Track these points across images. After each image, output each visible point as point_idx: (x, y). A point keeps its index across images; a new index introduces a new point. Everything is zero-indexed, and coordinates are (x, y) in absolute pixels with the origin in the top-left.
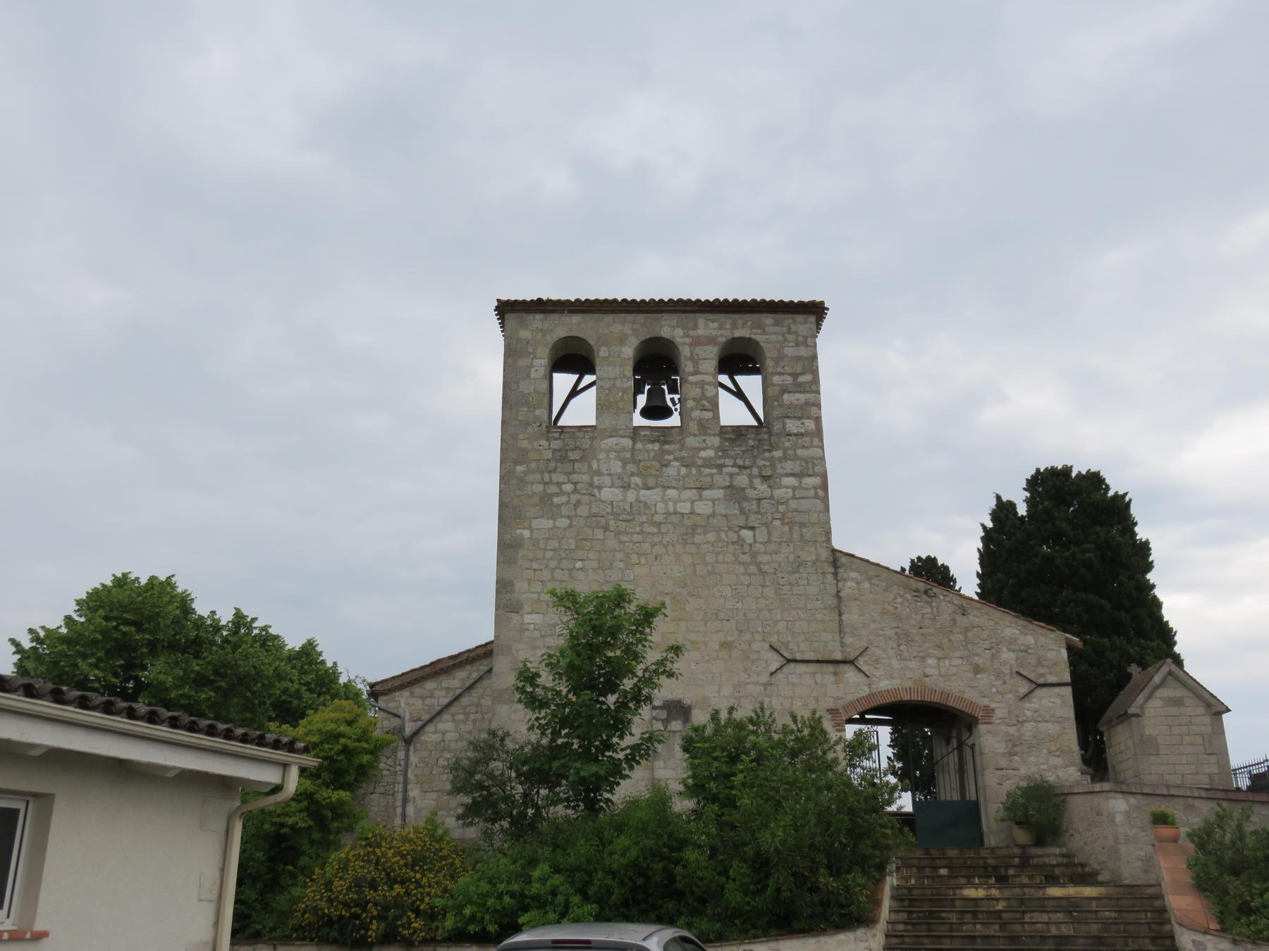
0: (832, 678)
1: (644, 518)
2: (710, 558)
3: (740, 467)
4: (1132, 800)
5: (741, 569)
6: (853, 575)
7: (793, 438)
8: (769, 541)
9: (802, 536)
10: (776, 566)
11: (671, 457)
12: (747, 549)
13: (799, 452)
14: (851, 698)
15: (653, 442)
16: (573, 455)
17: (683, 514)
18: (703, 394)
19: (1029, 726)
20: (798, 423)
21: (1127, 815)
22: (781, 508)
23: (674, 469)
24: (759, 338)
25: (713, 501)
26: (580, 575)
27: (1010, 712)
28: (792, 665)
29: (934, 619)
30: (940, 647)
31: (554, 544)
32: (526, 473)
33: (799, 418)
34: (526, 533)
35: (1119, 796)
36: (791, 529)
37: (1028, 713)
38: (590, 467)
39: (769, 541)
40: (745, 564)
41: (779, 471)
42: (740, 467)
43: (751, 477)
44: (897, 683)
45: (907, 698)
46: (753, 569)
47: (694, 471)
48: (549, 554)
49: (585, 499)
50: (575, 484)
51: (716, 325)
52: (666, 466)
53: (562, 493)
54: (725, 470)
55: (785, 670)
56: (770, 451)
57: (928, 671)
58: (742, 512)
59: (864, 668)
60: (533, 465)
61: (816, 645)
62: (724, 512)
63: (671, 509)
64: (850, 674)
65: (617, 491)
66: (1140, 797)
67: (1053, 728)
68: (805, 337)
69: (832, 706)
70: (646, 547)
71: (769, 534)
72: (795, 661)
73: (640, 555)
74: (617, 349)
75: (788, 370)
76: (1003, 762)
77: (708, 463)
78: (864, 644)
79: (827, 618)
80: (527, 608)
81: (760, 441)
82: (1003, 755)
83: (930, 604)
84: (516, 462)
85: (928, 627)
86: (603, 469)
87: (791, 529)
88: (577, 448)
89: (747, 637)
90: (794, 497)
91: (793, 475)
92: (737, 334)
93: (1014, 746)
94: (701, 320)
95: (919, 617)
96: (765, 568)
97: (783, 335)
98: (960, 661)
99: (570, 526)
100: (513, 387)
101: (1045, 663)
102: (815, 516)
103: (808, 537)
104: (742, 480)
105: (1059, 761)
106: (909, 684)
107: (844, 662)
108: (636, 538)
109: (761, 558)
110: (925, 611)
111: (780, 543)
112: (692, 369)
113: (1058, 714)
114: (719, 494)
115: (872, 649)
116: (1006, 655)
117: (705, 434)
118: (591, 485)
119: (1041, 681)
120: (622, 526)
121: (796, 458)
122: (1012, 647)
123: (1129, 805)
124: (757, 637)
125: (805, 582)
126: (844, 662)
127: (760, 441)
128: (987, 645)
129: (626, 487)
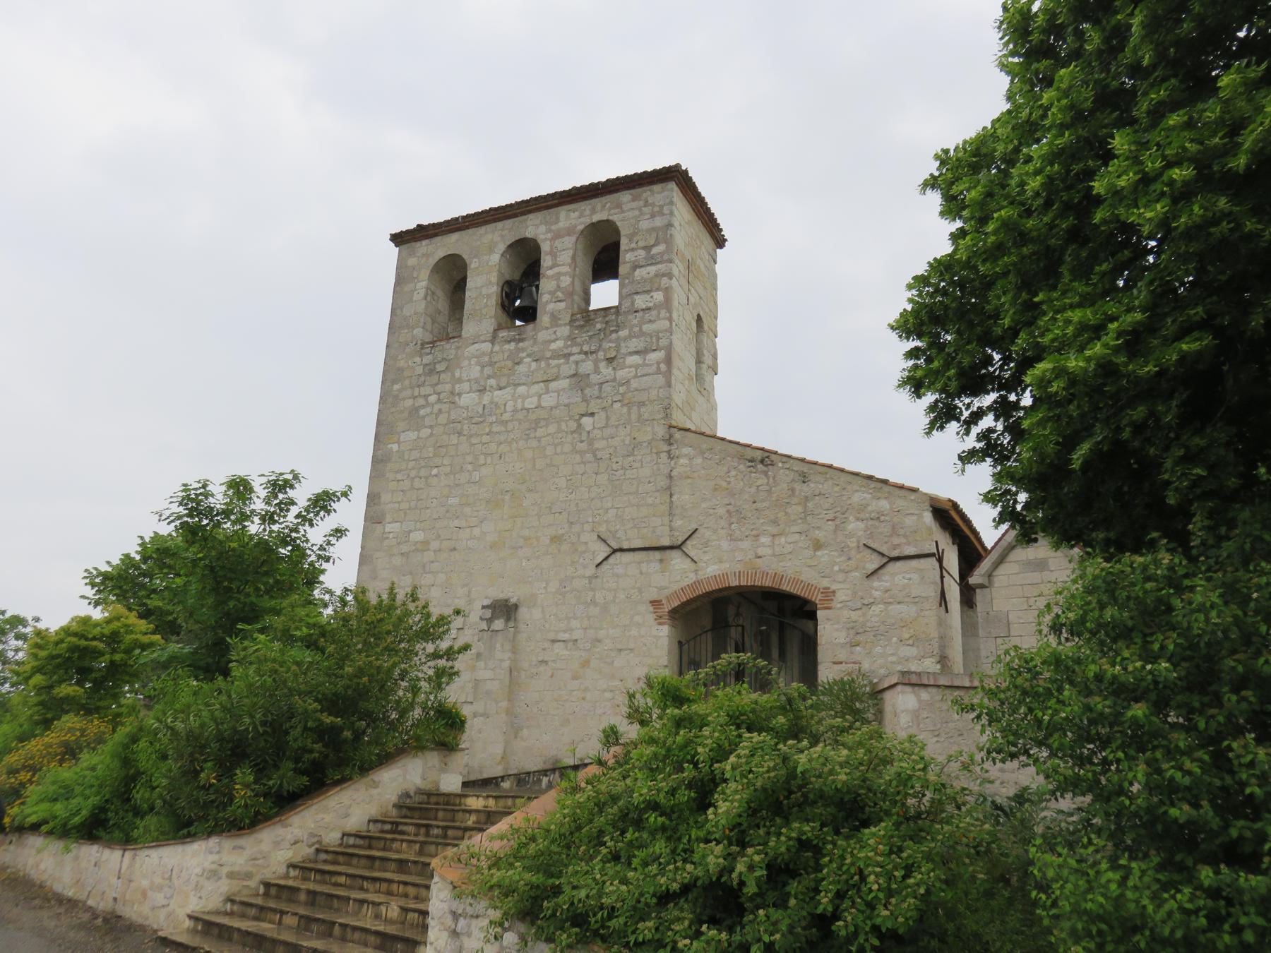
0: (658, 566)
1: (494, 418)
2: (549, 451)
3: (586, 353)
4: (924, 695)
5: (578, 458)
6: (685, 450)
7: (640, 314)
8: (607, 426)
9: (640, 416)
10: (611, 451)
11: (524, 355)
12: (584, 437)
13: (646, 327)
14: (676, 587)
15: (509, 342)
16: (439, 368)
17: (528, 410)
18: (558, 286)
19: (876, 609)
20: (647, 297)
21: (916, 714)
22: (622, 390)
23: (527, 366)
24: (614, 218)
25: (558, 392)
26: (434, 481)
27: (855, 593)
28: (618, 554)
29: (769, 491)
30: (775, 522)
31: (415, 454)
32: (400, 391)
33: (648, 292)
34: (395, 447)
35: (908, 689)
36: (629, 409)
37: (877, 594)
38: (453, 375)
39: (607, 426)
40: (582, 453)
41: (623, 350)
42: (586, 353)
43: (596, 363)
44: (725, 567)
45: (734, 583)
46: (589, 456)
47: (543, 364)
48: (411, 464)
49: (445, 407)
50: (439, 394)
51: (577, 213)
52: (518, 364)
53: (428, 404)
54: (572, 358)
55: (611, 560)
56: (616, 331)
57: (761, 551)
58: (585, 400)
59: (692, 554)
60: (407, 382)
61: (645, 531)
62: (566, 401)
63: (519, 406)
64: (676, 559)
65: (473, 395)
66: (934, 690)
67: (907, 611)
68: (661, 207)
69: (655, 597)
70: (493, 446)
71: (608, 418)
72: (621, 550)
73: (486, 455)
74: (486, 258)
75: (641, 244)
76: (842, 655)
77: (557, 355)
78: (694, 526)
79: (658, 501)
80: (389, 518)
81: (607, 323)
82: (843, 646)
83: (766, 474)
84: (394, 382)
85: (763, 501)
86: (464, 377)
87: (629, 409)
88: (444, 359)
89: (576, 528)
90: (636, 376)
91: (637, 353)
92: (596, 218)
93: (857, 635)
94: (563, 211)
95: (753, 490)
96: (599, 454)
97: (640, 209)
98: (797, 537)
99: (431, 434)
100: (398, 312)
101: (901, 532)
102: (655, 392)
103: (646, 416)
104: (587, 367)
105: (912, 651)
106: (739, 567)
107: (671, 548)
108: (485, 439)
109: (597, 445)
110: (760, 482)
111: (617, 427)
112: (550, 263)
113: (915, 593)
114: (564, 383)
115: (701, 530)
116: (853, 526)
117: (557, 326)
118: (452, 393)
119: (895, 554)
120: (474, 428)
121: (642, 334)
122: (862, 516)
123: (920, 701)
124: (587, 527)
125: (638, 465)
126: (671, 548)
127: (607, 323)
128: (831, 516)
129: (482, 391)
